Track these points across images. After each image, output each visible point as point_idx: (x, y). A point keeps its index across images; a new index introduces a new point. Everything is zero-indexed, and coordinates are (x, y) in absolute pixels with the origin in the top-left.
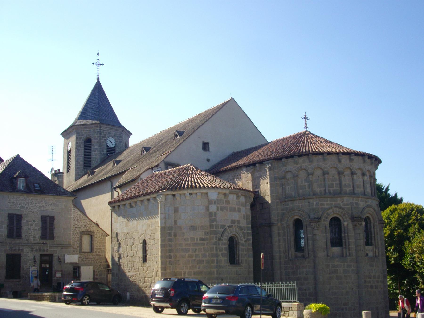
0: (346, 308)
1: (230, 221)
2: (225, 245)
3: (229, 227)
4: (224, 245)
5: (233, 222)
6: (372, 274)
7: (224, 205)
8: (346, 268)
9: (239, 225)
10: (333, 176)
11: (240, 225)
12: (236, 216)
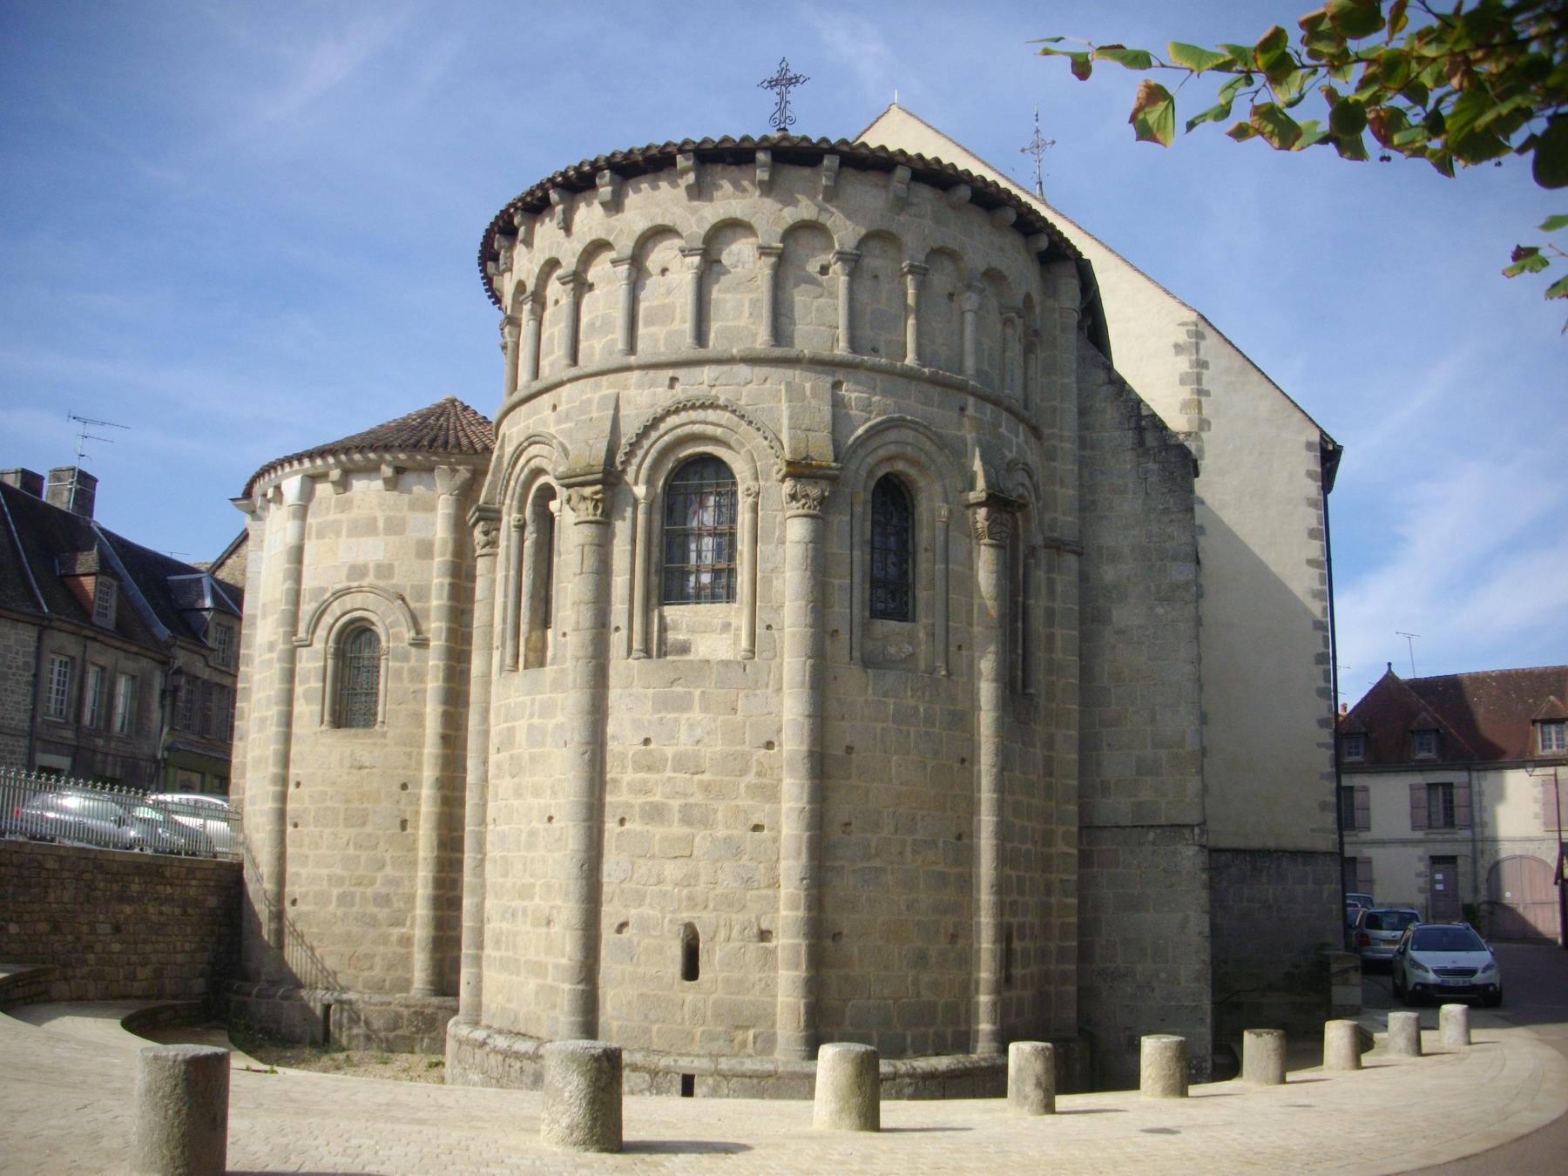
0: (524, 910)
1: (344, 572)
2: (316, 660)
3: (338, 595)
4: (314, 662)
5: (357, 571)
6: (670, 751)
7: (332, 517)
8: (536, 721)
9: (382, 583)
10: (557, 302)
11: (394, 581)
12: (372, 550)
